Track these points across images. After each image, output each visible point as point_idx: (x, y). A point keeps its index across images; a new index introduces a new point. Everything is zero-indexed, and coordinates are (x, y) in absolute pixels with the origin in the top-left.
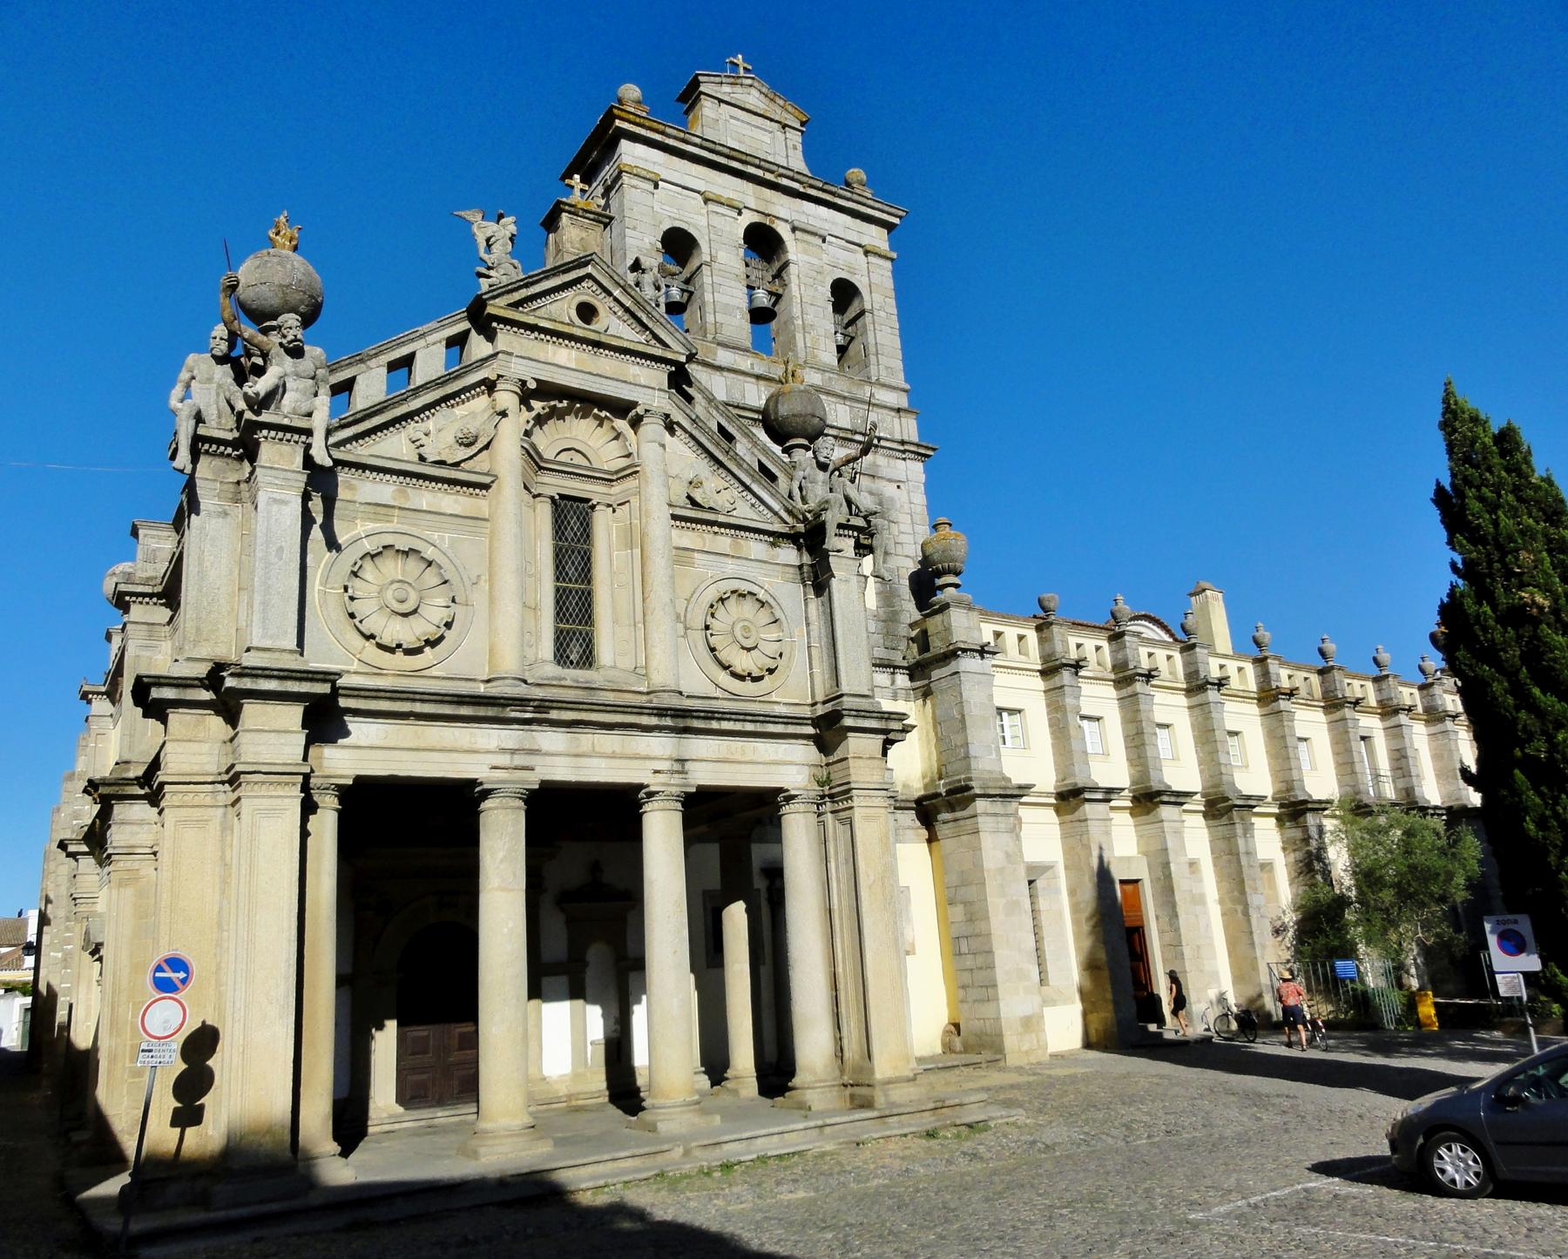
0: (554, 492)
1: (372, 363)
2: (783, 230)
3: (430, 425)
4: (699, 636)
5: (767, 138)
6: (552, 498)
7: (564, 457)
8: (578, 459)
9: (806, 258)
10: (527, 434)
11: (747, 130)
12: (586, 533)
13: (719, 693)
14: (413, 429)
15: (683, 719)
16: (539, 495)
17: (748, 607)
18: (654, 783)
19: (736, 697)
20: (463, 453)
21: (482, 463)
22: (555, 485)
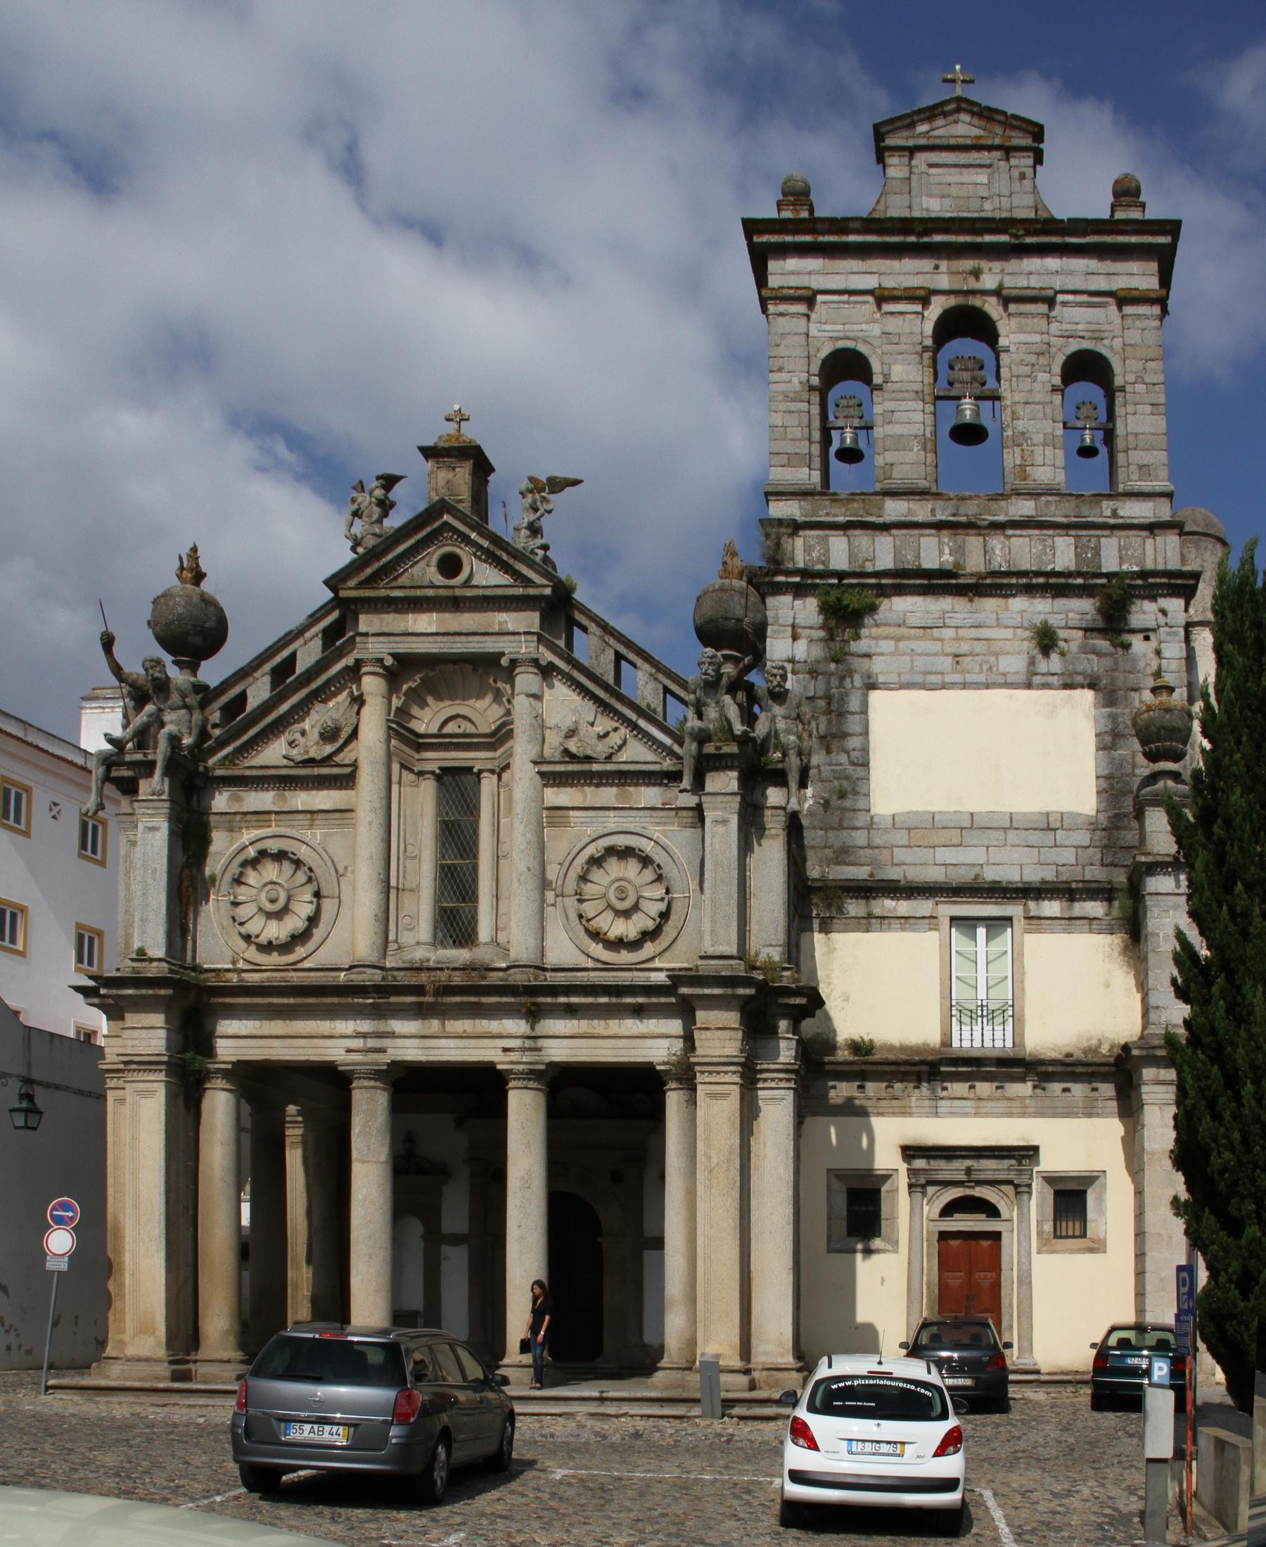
0: (434, 766)
1: (257, 675)
2: (992, 307)
3: (306, 724)
4: (571, 902)
5: (982, 177)
6: (433, 773)
7: (451, 728)
8: (470, 729)
9: (1022, 337)
10: (403, 712)
11: (953, 176)
12: (472, 809)
13: (590, 964)
14: (293, 733)
15: (536, 996)
16: (421, 774)
17: (631, 869)
18: (502, 1061)
19: (608, 967)
20: (328, 749)
21: (346, 757)
22: (434, 760)
